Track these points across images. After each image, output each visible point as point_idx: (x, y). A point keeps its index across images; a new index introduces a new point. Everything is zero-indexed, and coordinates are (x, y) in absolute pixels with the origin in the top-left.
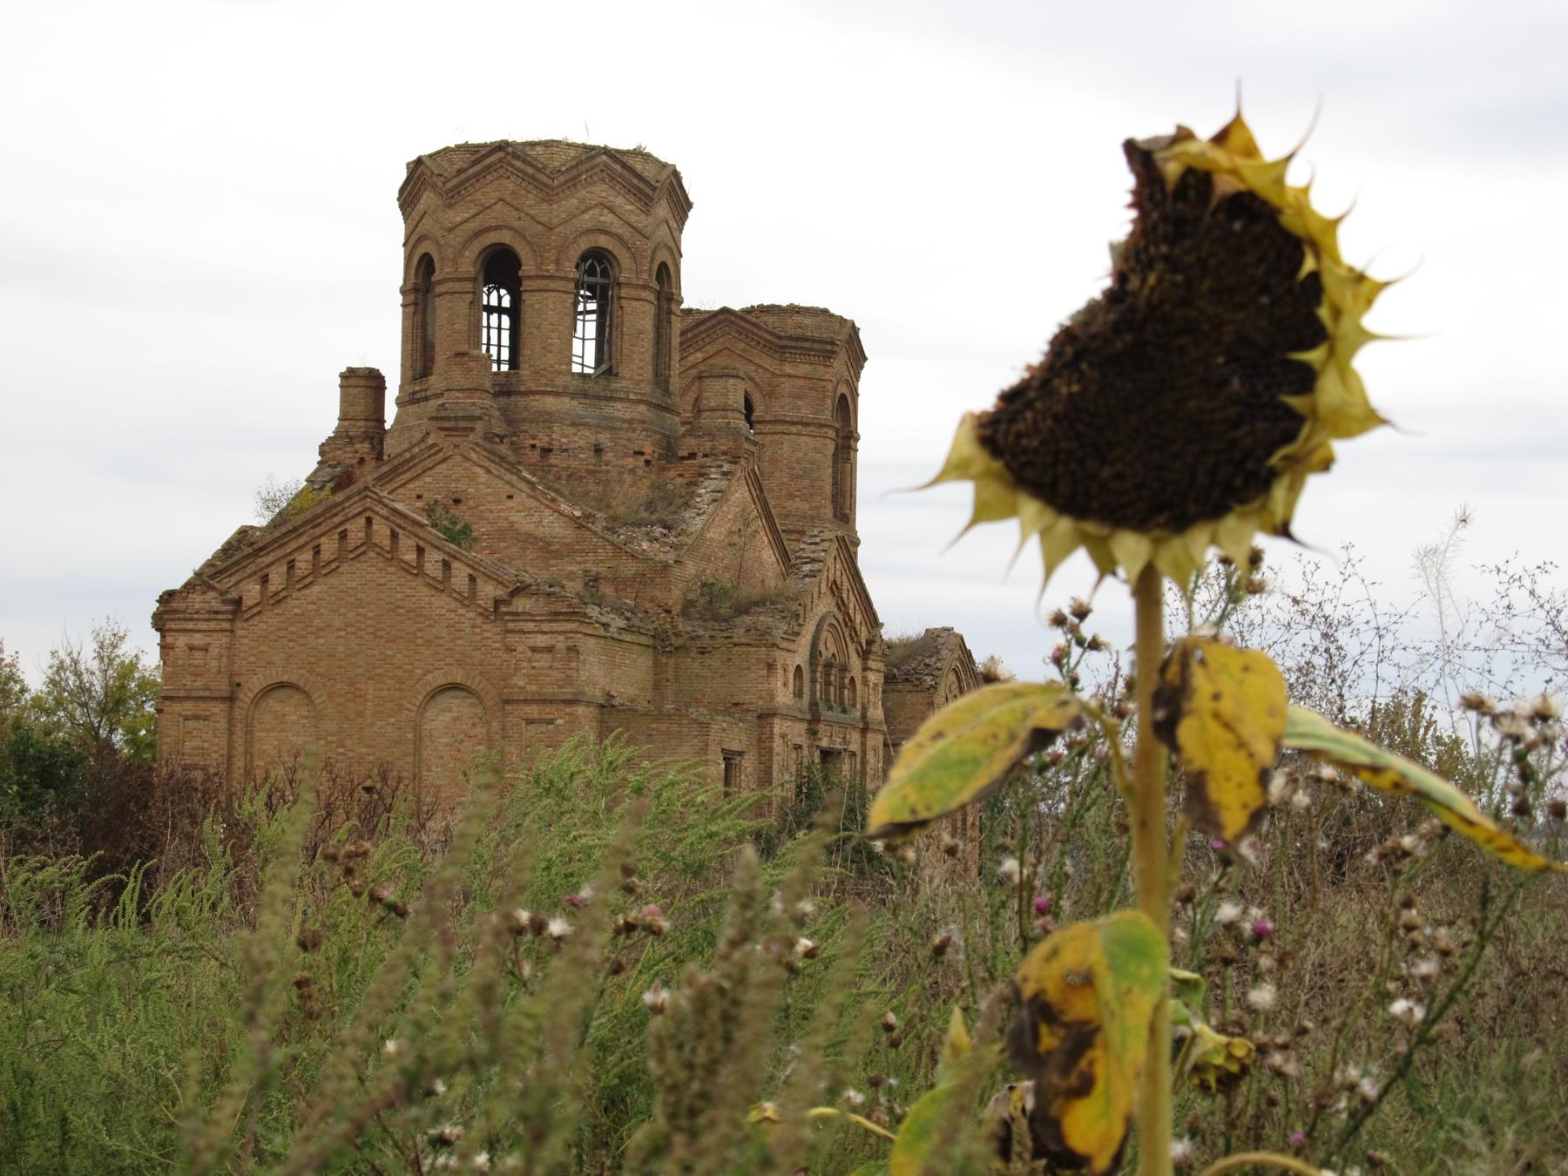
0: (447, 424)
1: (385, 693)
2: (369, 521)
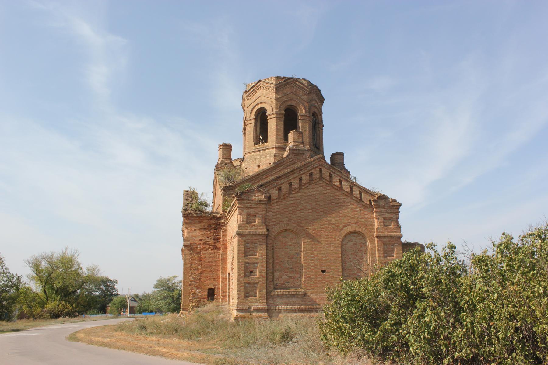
0: (295, 152)
2: (321, 170)
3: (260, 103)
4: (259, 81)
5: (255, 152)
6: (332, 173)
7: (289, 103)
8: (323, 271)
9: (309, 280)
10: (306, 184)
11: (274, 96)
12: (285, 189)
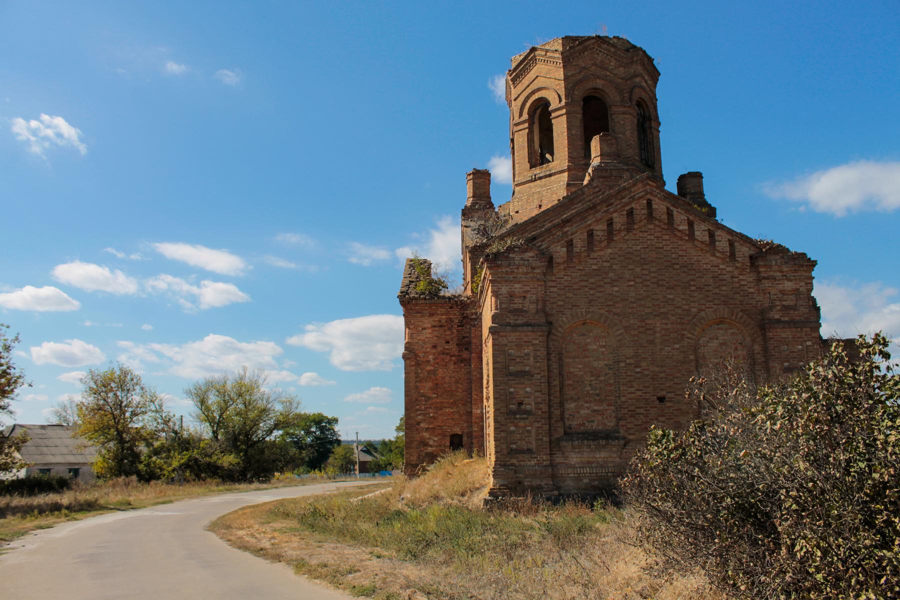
1: (669, 326)
2: (649, 203)
3: (539, 89)
4: (533, 50)
5: (531, 181)
6: (671, 208)
7: (590, 84)
8: (661, 399)
9: (632, 416)
10: (620, 231)
11: (560, 74)
12: (579, 243)
